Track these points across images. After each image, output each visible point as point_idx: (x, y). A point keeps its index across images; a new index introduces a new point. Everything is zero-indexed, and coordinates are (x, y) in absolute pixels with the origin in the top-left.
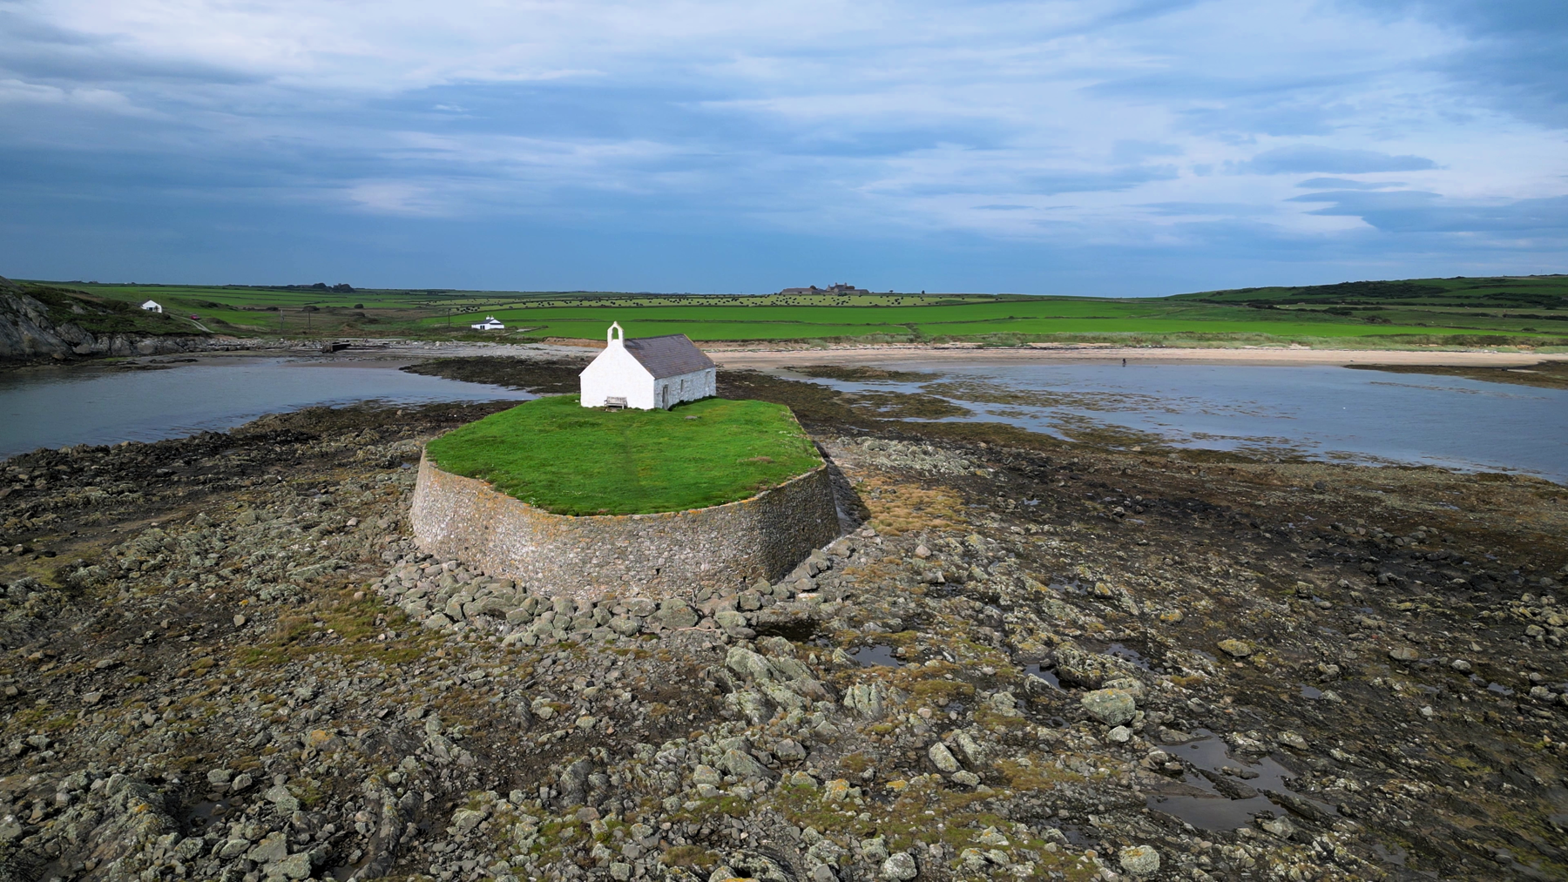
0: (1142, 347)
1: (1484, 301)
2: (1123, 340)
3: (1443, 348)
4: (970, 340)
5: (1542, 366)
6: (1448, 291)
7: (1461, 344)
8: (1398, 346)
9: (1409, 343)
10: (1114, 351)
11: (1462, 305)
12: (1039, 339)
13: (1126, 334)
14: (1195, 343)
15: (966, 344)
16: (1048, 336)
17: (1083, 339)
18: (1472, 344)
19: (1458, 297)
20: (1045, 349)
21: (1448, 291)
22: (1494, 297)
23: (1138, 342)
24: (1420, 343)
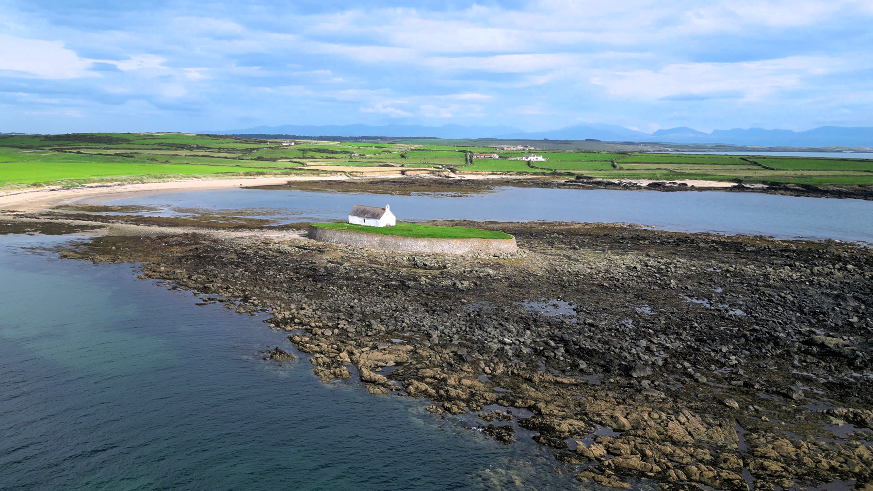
0: (136, 183)
1: (156, 147)
2: (124, 180)
3: (245, 177)
4: (55, 184)
5: (290, 183)
6: (133, 141)
7: (250, 175)
8: (231, 177)
9: (233, 175)
10: (124, 187)
11: (153, 149)
12: (86, 181)
13: (124, 177)
14: (157, 180)
15: (58, 187)
16: (90, 180)
17: (108, 181)
18: (254, 175)
19: (143, 144)
20: (97, 187)
21: (133, 141)
22: (159, 144)
23: (132, 181)
24: (237, 175)
